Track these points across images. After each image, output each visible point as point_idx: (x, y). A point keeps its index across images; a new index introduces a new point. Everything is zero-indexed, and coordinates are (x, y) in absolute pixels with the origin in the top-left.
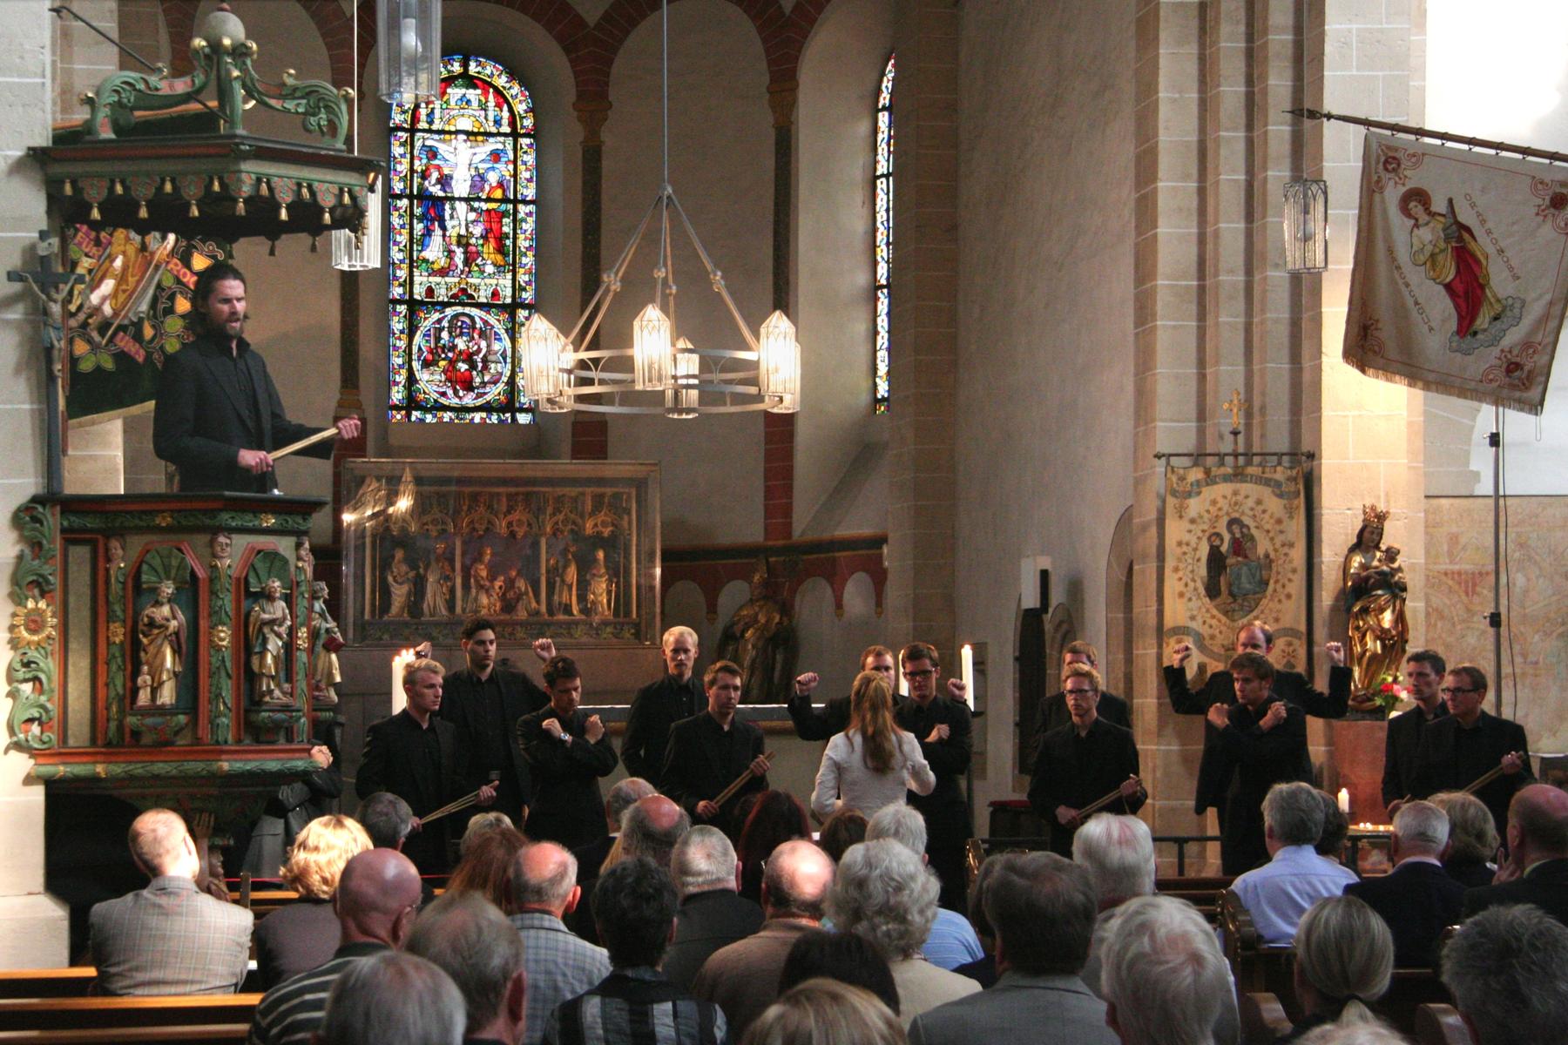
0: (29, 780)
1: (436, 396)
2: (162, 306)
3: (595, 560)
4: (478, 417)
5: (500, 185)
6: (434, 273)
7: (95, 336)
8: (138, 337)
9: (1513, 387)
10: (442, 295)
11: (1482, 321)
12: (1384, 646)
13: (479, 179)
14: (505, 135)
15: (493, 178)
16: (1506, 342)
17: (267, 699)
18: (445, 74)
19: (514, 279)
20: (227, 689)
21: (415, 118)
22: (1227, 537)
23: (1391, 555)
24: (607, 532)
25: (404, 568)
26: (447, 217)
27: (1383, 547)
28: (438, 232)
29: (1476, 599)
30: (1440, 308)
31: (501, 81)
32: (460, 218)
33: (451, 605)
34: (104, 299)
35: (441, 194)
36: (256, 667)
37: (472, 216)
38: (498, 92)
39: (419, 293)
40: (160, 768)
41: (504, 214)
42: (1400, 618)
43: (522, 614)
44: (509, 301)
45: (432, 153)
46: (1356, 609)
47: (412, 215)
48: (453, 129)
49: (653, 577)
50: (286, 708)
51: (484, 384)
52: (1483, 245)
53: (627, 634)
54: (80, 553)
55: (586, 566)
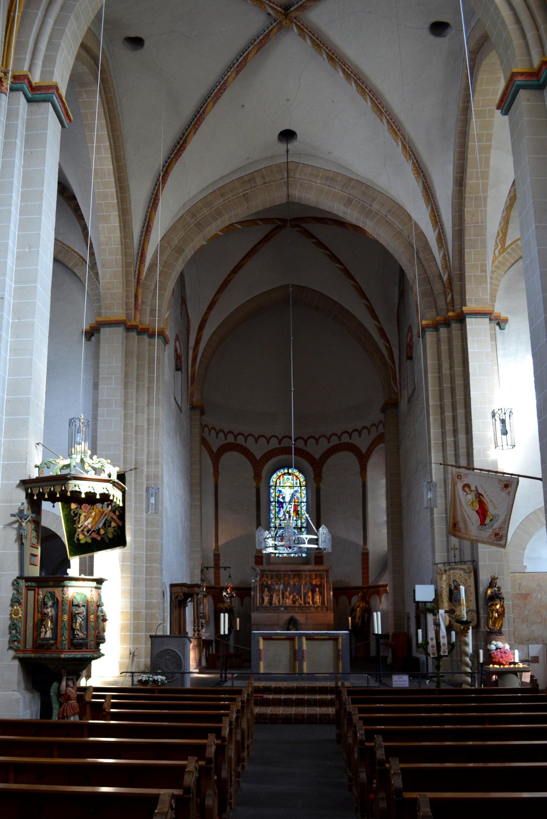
0: (14, 658)
2: (106, 525)
3: (316, 591)
4: (292, 555)
7: (86, 533)
8: (98, 533)
9: (497, 540)
11: (487, 521)
12: (498, 615)
16: (494, 527)
17: (77, 636)
20: (66, 633)
21: (276, 483)
22: (453, 585)
23: (499, 588)
24: (318, 583)
25: (268, 593)
27: (497, 586)
29: (527, 601)
30: (475, 518)
31: (297, 474)
33: (279, 602)
34: (89, 524)
36: (74, 627)
38: (296, 476)
40: (47, 655)
42: (502, 606)
43: (297, 604)
46: (489, 604)
49: (330, 595)
50: (83, 639)
52: (486, 499)
53: (324, 610)
54: (31, 593)
55: (313, 592)
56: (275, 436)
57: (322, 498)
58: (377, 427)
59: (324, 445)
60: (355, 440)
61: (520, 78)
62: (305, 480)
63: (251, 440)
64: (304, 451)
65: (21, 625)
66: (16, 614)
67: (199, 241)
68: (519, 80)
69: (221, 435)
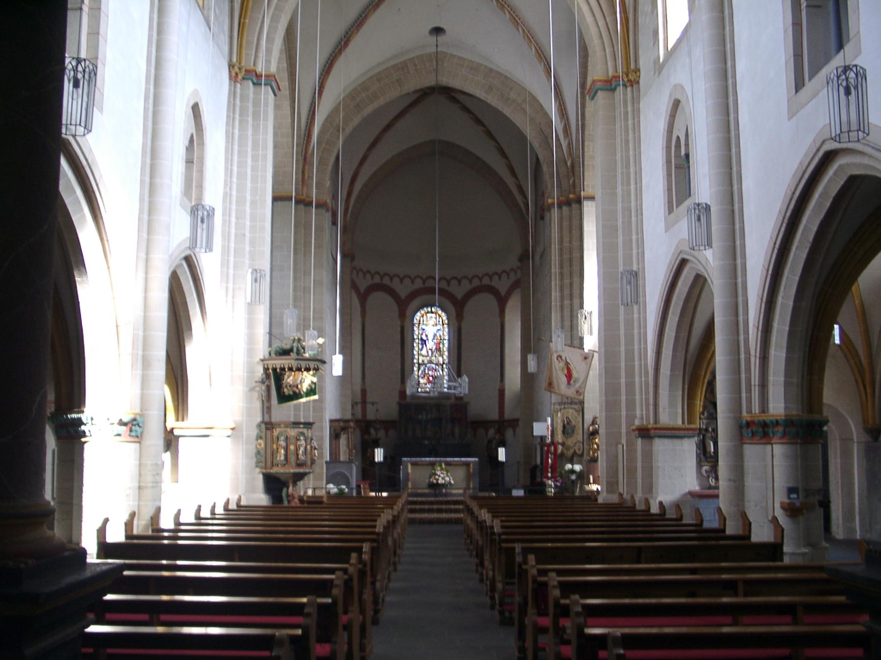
13: (435, 335)
31: (440, 312)
32: (431, 344)
56: (419, 277)
57: (463, 337)
58: (515, 272)
59: (466, 286)
60: (495, 283)
61: (599, 84)
62: (448, 319)
63: (396, 280)
64: (447, 291)
65: (263, 452)
66: (260, 445)
67: (356, 121)
68: (598, 85)
69: (368, 276)
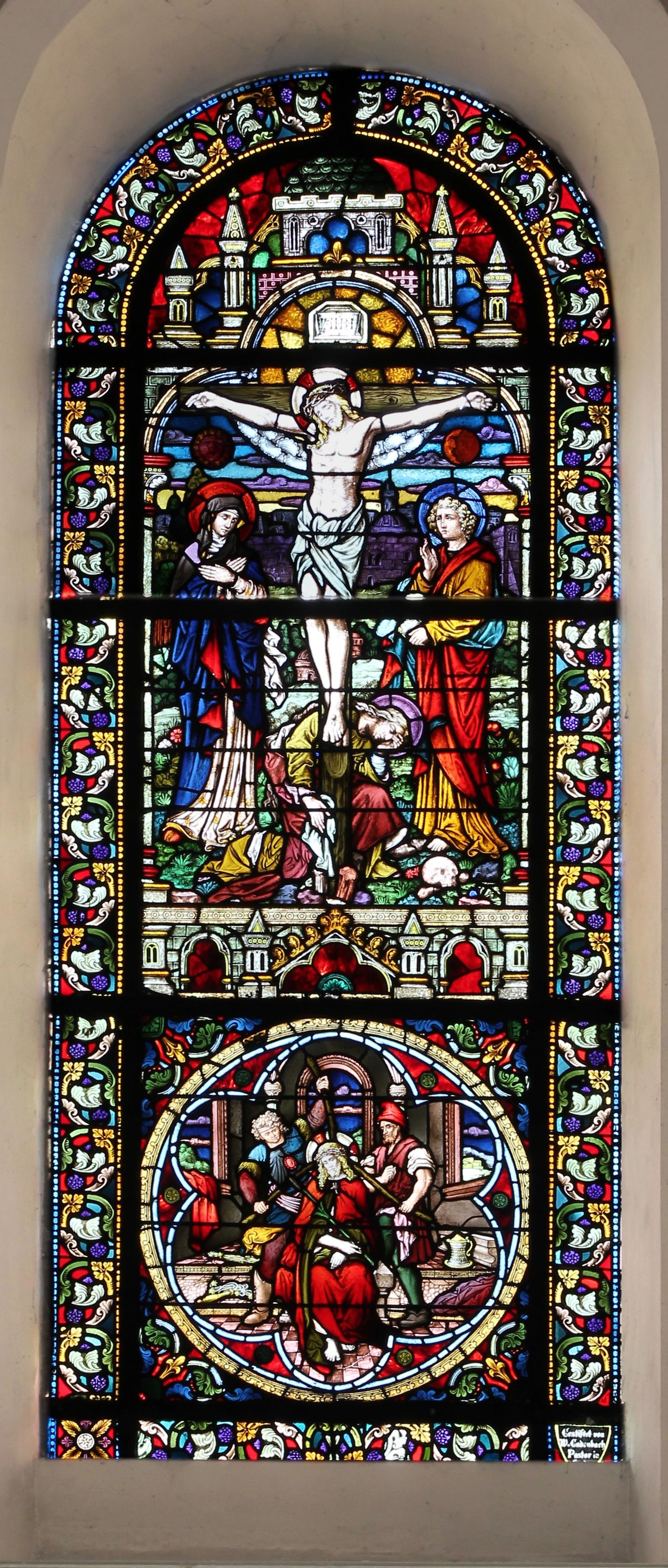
1: (229, 1361)
5: (481, 544)
6: (224, 893)
10: (252, 973)
13: (393, 531)
14: (499, 357)
15: (449, 520)
18: (261, 141)
19: (538, 909)
21: (148, 310)
26: (272, 676)
28: (238, 736)
35: (246, 591)
37: (368, 672)
38: (468, 197)
39: (163, 966)
41: (495, 660)
44: (517, 990)
45: (216, 439)
47: (136, 681)
48: (292, 342)
51: (423, 1313)
